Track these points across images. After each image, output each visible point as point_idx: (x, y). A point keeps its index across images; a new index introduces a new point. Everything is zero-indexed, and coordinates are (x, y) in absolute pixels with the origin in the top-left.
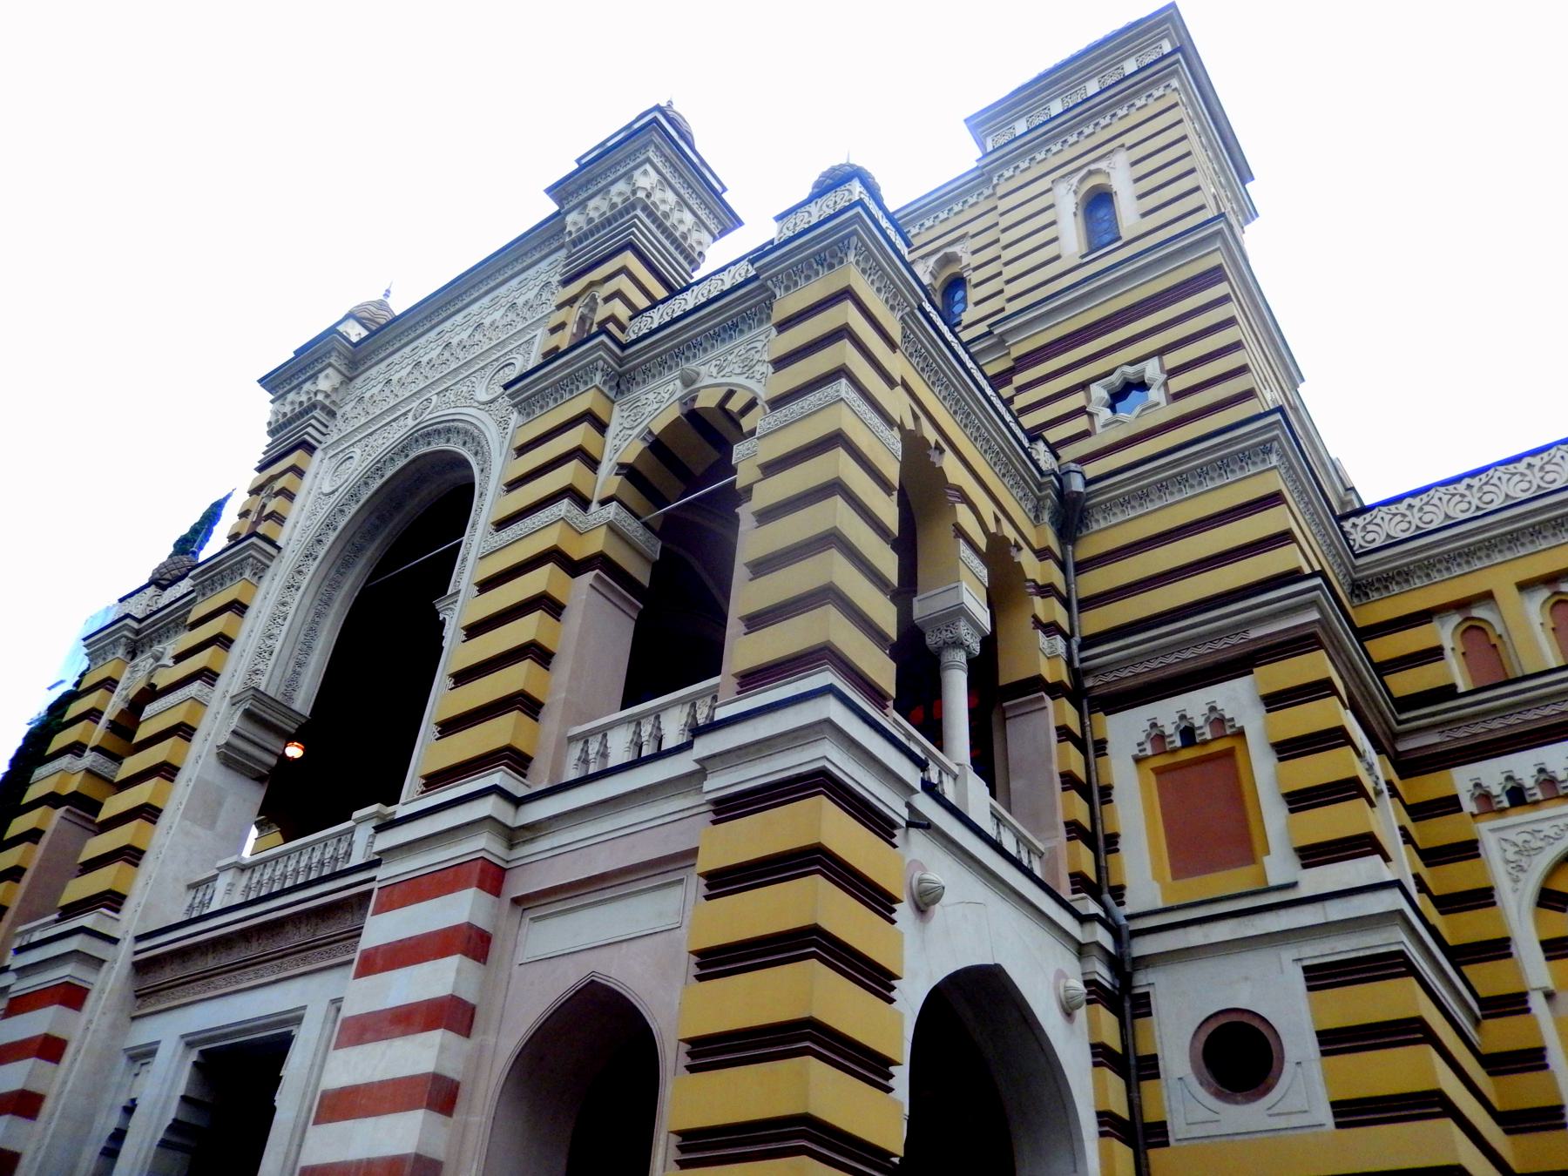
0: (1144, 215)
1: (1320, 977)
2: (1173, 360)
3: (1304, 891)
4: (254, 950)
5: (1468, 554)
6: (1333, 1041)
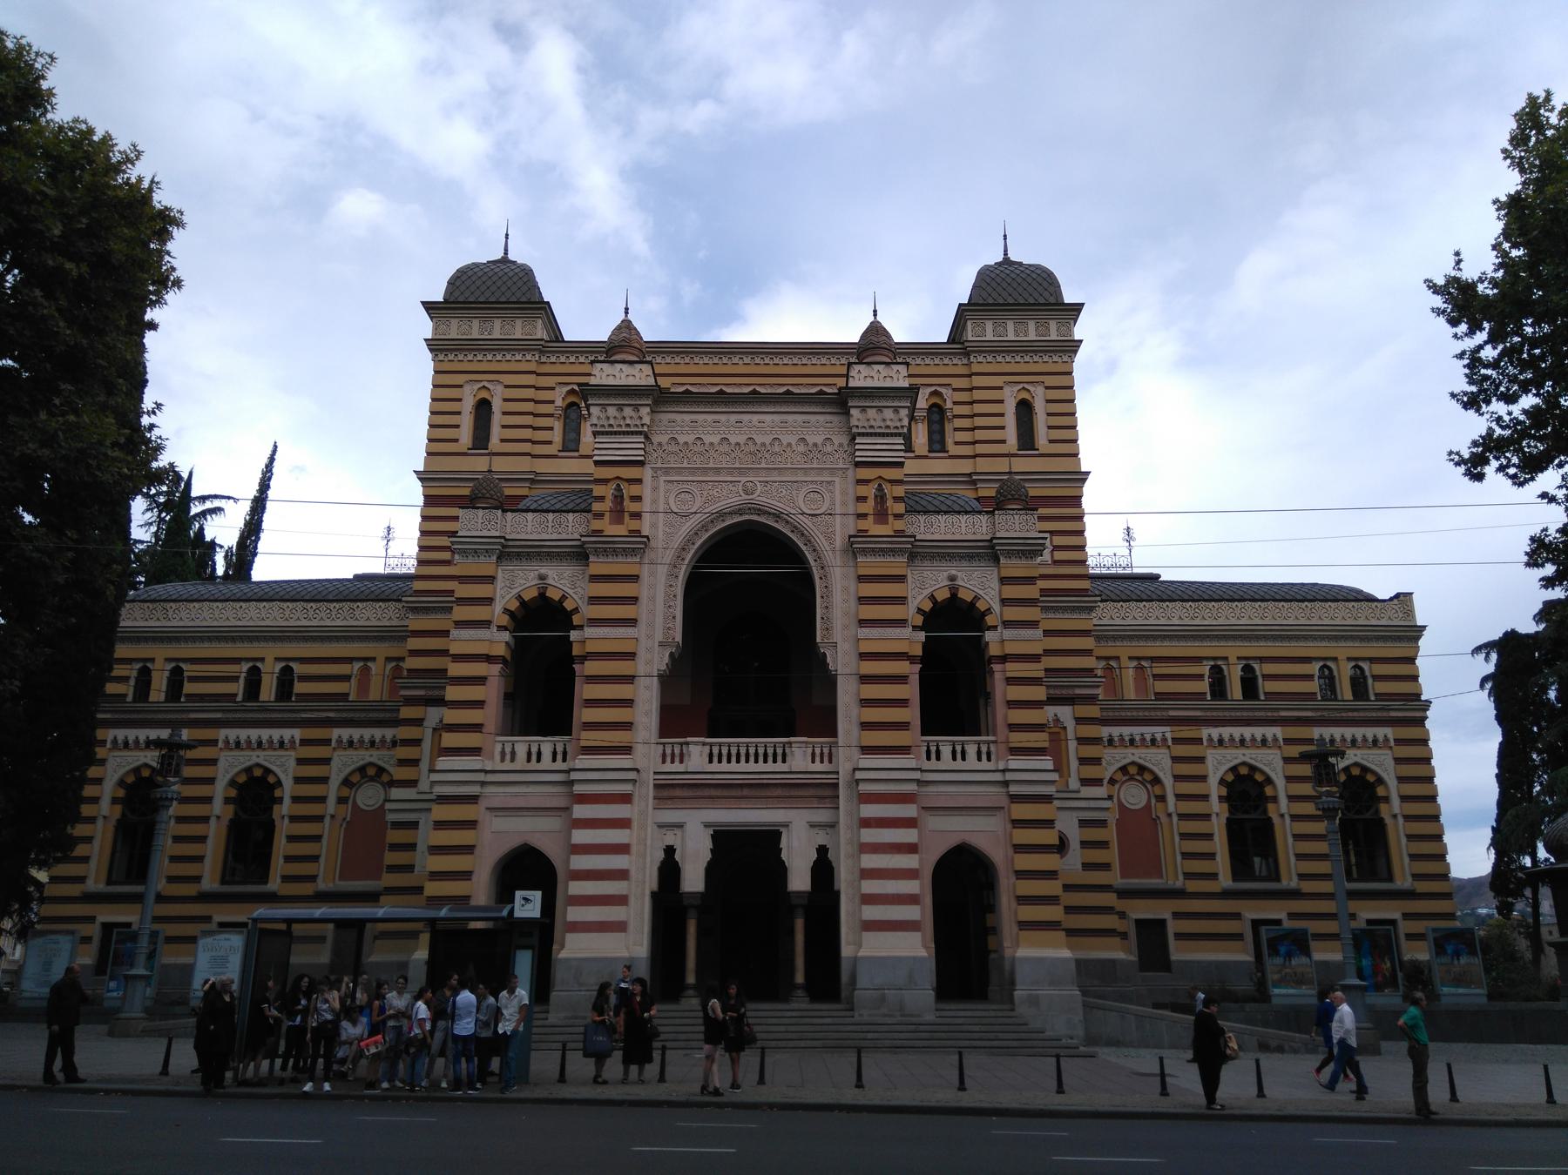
0: (1051, 441)
1: (1084, 823)
2: (1059, 541)
3: (1082, 795)
4: (746, 792)
5: (1115, 638)
6: (1085, 844)
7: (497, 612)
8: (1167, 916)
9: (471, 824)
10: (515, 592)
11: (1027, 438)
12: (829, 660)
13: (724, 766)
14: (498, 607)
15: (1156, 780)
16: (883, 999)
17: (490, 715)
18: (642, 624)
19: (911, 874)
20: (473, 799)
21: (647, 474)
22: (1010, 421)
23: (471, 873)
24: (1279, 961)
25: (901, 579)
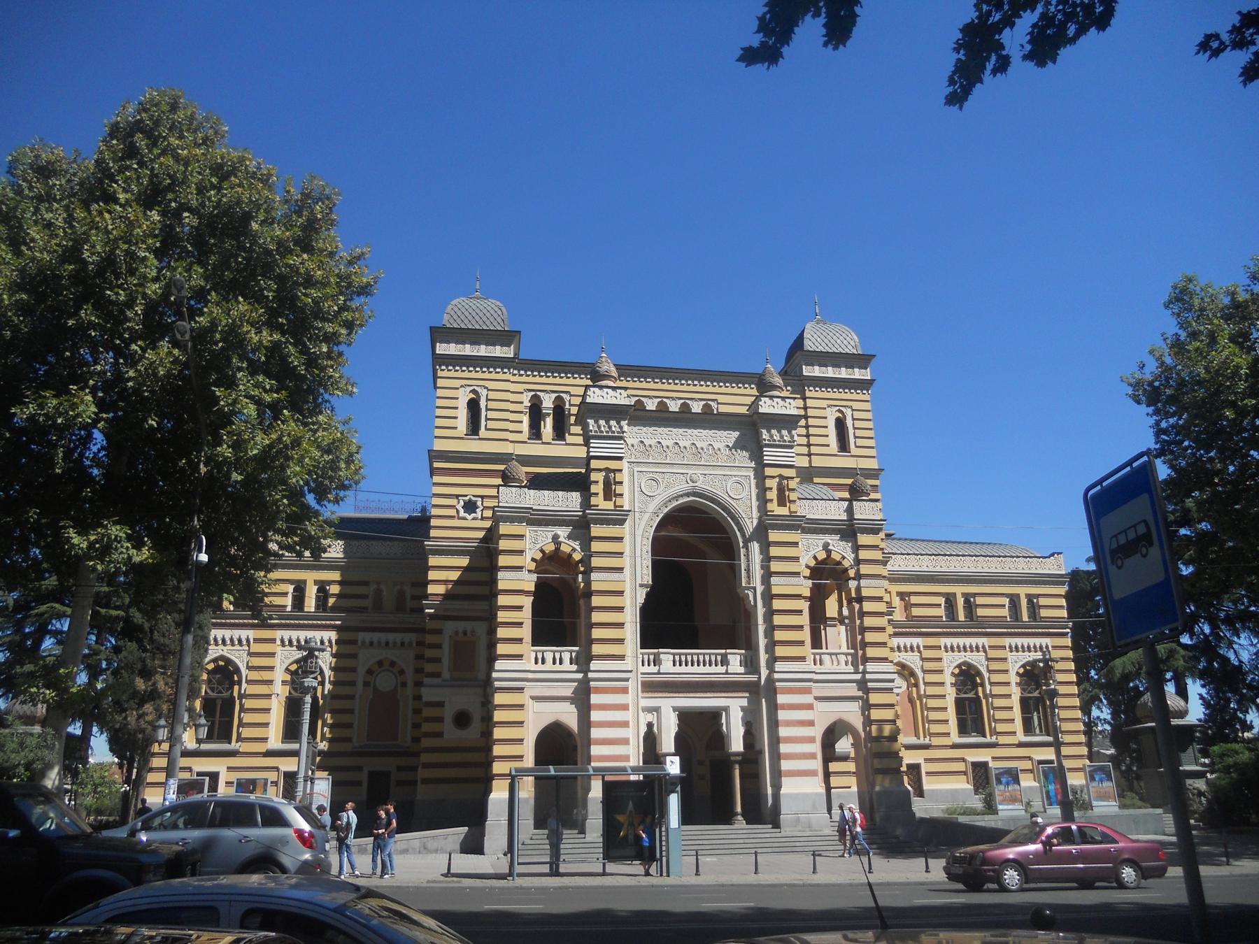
7: (527, 561)
8: (921, 761)
9: (520, 707)
10: (538, 546)
11: (843, 445)
12: (751, 598)
13: (683, 669)
14: (529, 559)
15: (912, 674)
16: (798, 820)
17: (526, 632)
18: (627, 571)
19: (811, 740)
20: (521, 689)
21: (624, 465)
22: (832, 431)
23: (522, 740)
24: (1002, 787)
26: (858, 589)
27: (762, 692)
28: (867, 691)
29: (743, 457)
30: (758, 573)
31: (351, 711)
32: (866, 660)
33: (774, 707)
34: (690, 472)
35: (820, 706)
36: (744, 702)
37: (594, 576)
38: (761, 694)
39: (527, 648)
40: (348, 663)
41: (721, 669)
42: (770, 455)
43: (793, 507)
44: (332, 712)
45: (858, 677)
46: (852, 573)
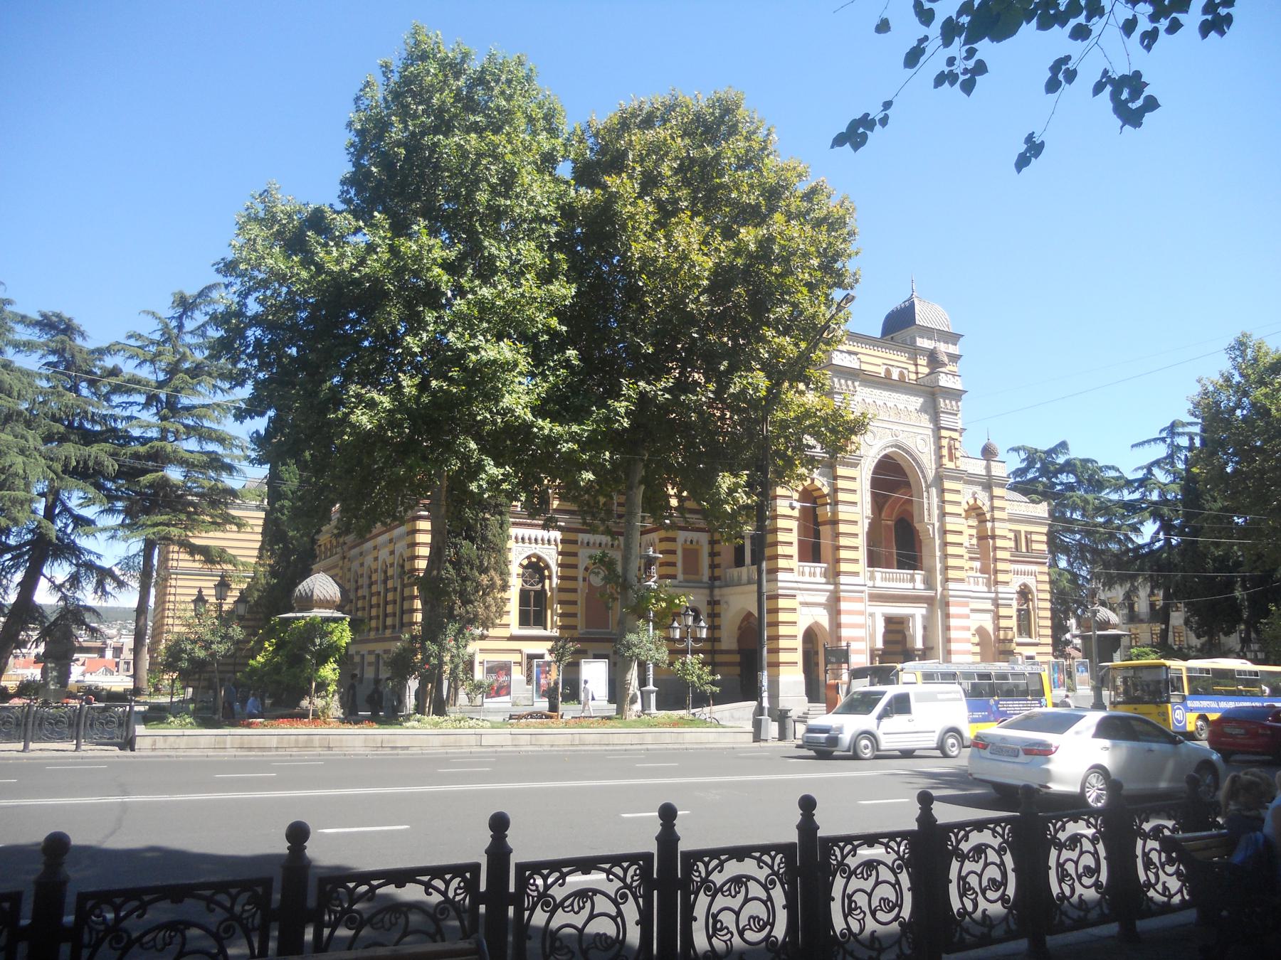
25: (958, 492)
26: (993, 529)
27: (937, 603)
28: (997, 606)
29: (925, 420)
30: (936, 512)
31: (575, 603)
32: (996, 583)
33: (947, 616)
34: (895, 427)
35: (974, 616)
36: (924, 611)
37: (841, 508)
38: (938, 605)
39: (794, 563)
40: (570, 560)
41: (910, 586)
42: (945, 420)
43: (958, 463)
44: (560, 602)
45: (993, 595)
46: (988, 516)
